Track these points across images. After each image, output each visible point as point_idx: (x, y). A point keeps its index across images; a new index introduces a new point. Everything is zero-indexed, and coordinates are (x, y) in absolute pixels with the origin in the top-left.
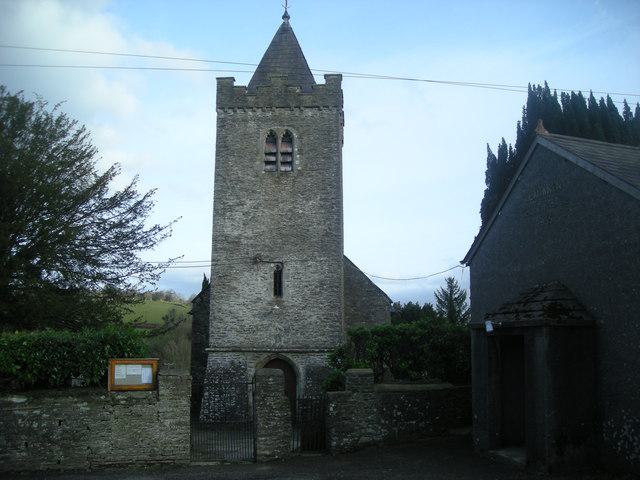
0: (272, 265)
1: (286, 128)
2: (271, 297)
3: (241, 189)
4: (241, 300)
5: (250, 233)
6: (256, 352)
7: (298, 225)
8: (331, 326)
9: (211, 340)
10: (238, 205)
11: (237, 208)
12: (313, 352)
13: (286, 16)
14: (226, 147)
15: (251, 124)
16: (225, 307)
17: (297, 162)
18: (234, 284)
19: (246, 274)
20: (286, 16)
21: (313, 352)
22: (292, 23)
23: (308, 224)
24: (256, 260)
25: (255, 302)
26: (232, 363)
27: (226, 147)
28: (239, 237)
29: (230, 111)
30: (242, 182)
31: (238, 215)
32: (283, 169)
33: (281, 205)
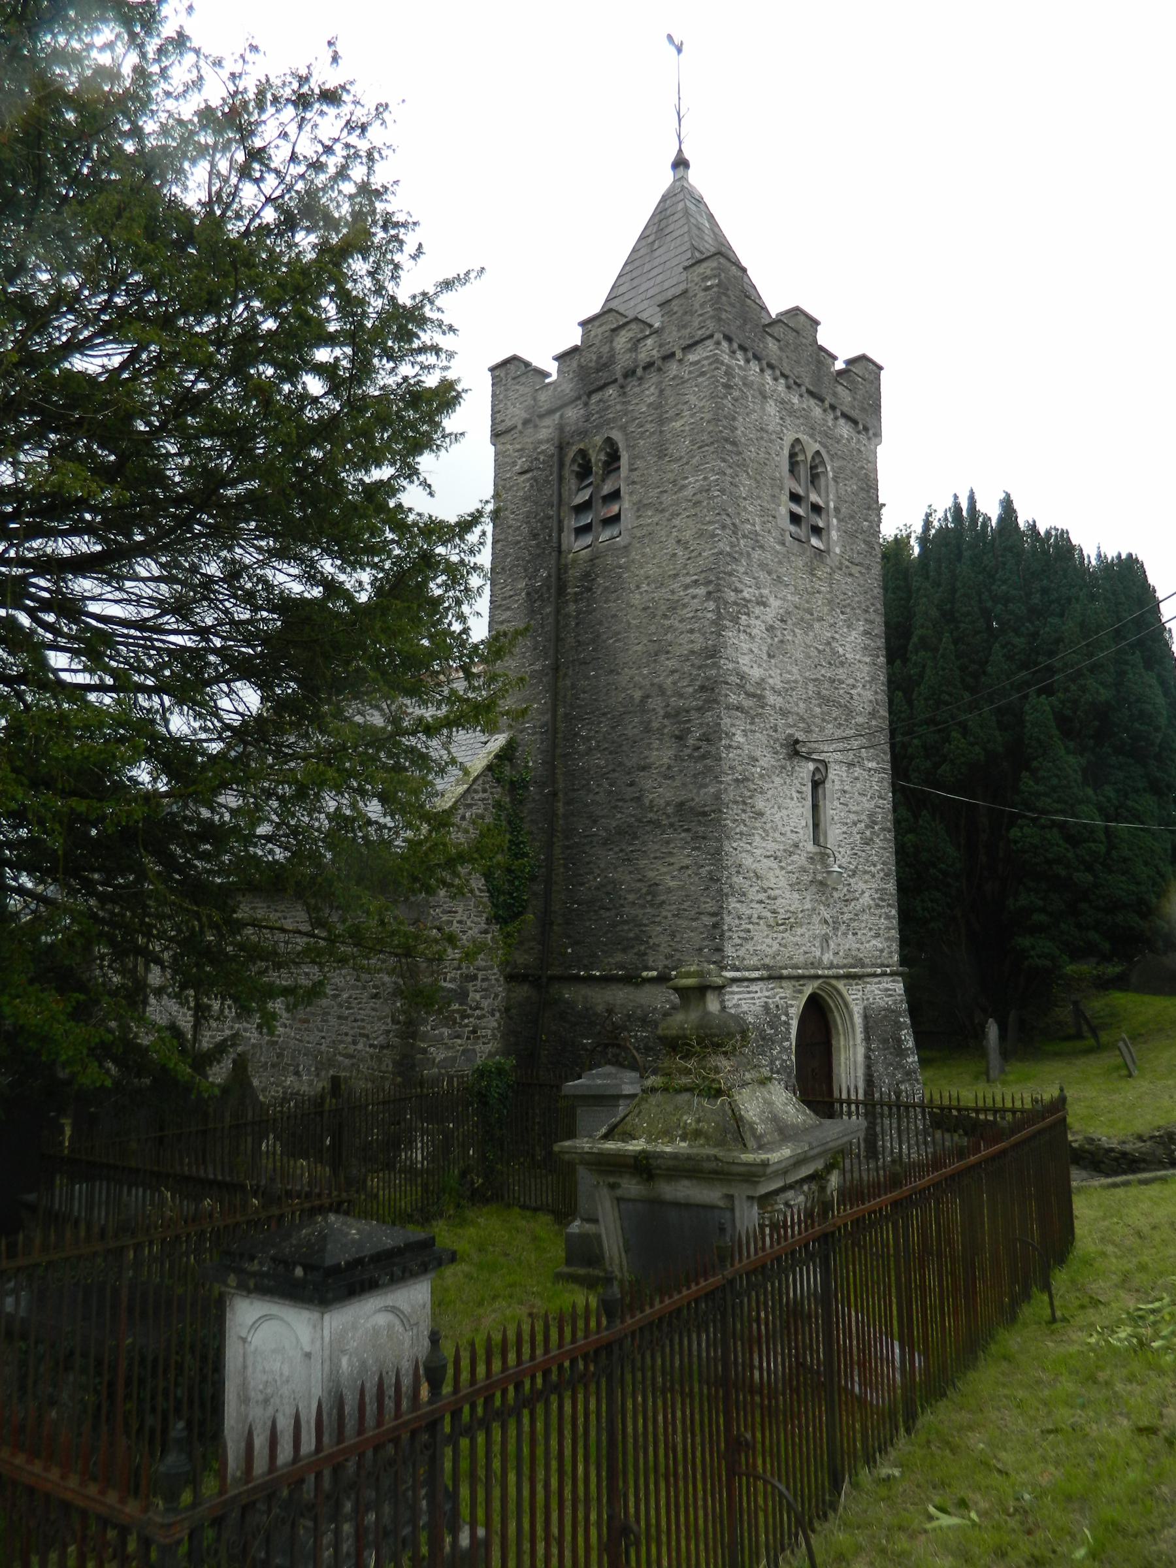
0: (811, 766)
1: (817, 447)
2: (810, 847)
3: (762, 566)
4: (772, 846)
5: (776, 681)
6: (799, 978)
7: (842, 682)
8: (888, 917)
9: (729, 950)
10: (758, 603)
11: (758, 610)
12: (875, 975)
13: (680, 163)
14: (734, 443)
15: (771, 408)
16: (748, 861)
17: (834, 535)
18: (760, 804)
19: (778, 781)
20: (680, 163)
21: (875, 975)
22: (696, 178)
23: (851, 681)
24: (794, 750)
25: (791, 854)
26: (766, 1007)
27: (734, 443)
28: (761, 683)
29: (740, 355)
30: (762, 547)
31: (758, 629)
32: (814, 541)
33: (817, 625)
